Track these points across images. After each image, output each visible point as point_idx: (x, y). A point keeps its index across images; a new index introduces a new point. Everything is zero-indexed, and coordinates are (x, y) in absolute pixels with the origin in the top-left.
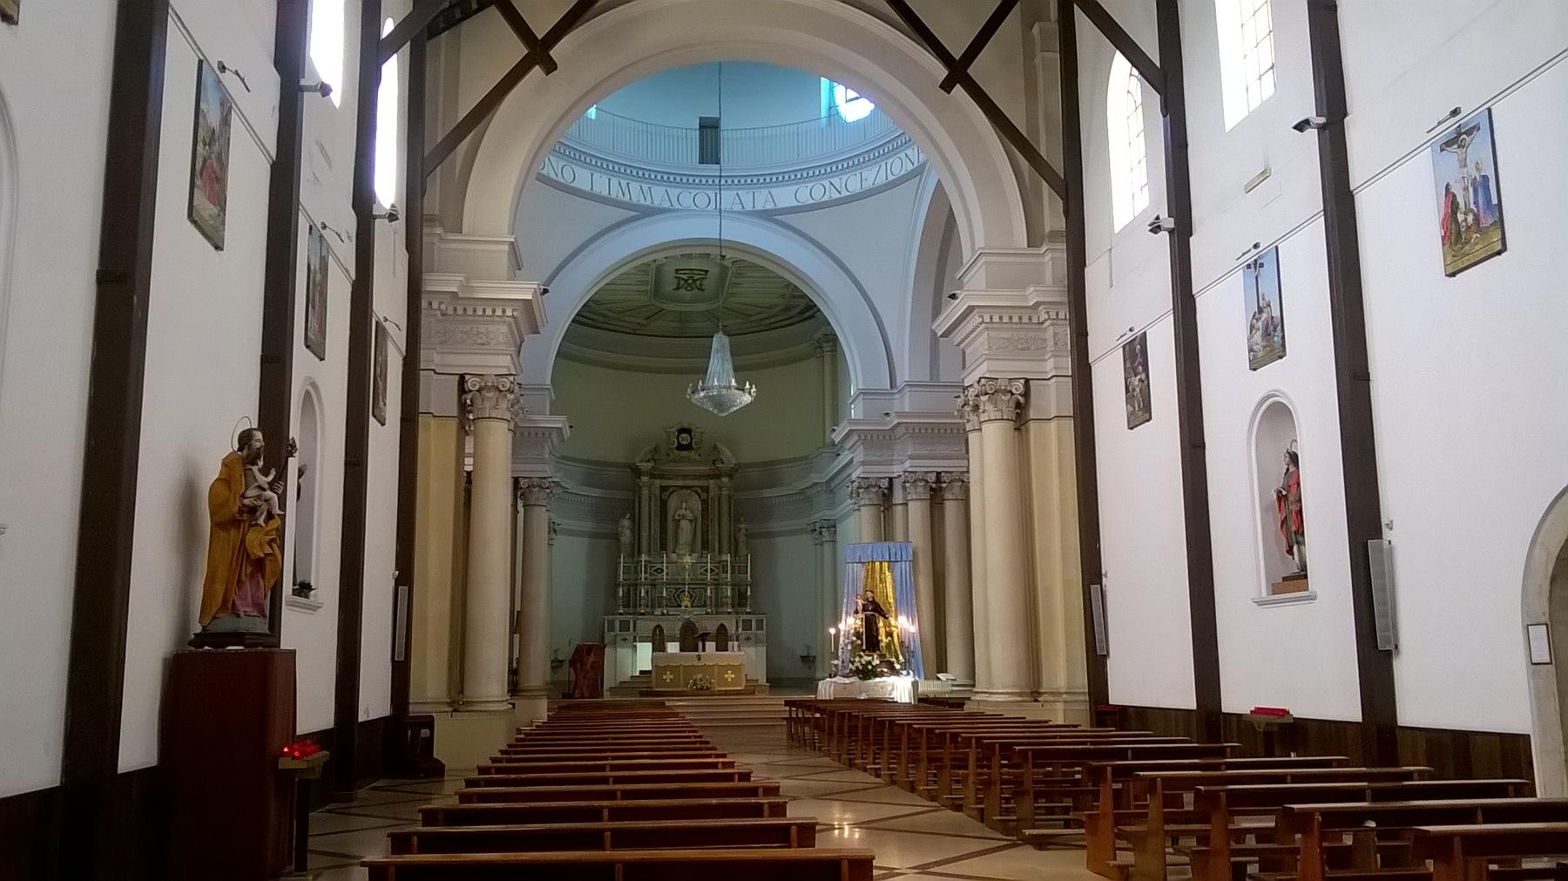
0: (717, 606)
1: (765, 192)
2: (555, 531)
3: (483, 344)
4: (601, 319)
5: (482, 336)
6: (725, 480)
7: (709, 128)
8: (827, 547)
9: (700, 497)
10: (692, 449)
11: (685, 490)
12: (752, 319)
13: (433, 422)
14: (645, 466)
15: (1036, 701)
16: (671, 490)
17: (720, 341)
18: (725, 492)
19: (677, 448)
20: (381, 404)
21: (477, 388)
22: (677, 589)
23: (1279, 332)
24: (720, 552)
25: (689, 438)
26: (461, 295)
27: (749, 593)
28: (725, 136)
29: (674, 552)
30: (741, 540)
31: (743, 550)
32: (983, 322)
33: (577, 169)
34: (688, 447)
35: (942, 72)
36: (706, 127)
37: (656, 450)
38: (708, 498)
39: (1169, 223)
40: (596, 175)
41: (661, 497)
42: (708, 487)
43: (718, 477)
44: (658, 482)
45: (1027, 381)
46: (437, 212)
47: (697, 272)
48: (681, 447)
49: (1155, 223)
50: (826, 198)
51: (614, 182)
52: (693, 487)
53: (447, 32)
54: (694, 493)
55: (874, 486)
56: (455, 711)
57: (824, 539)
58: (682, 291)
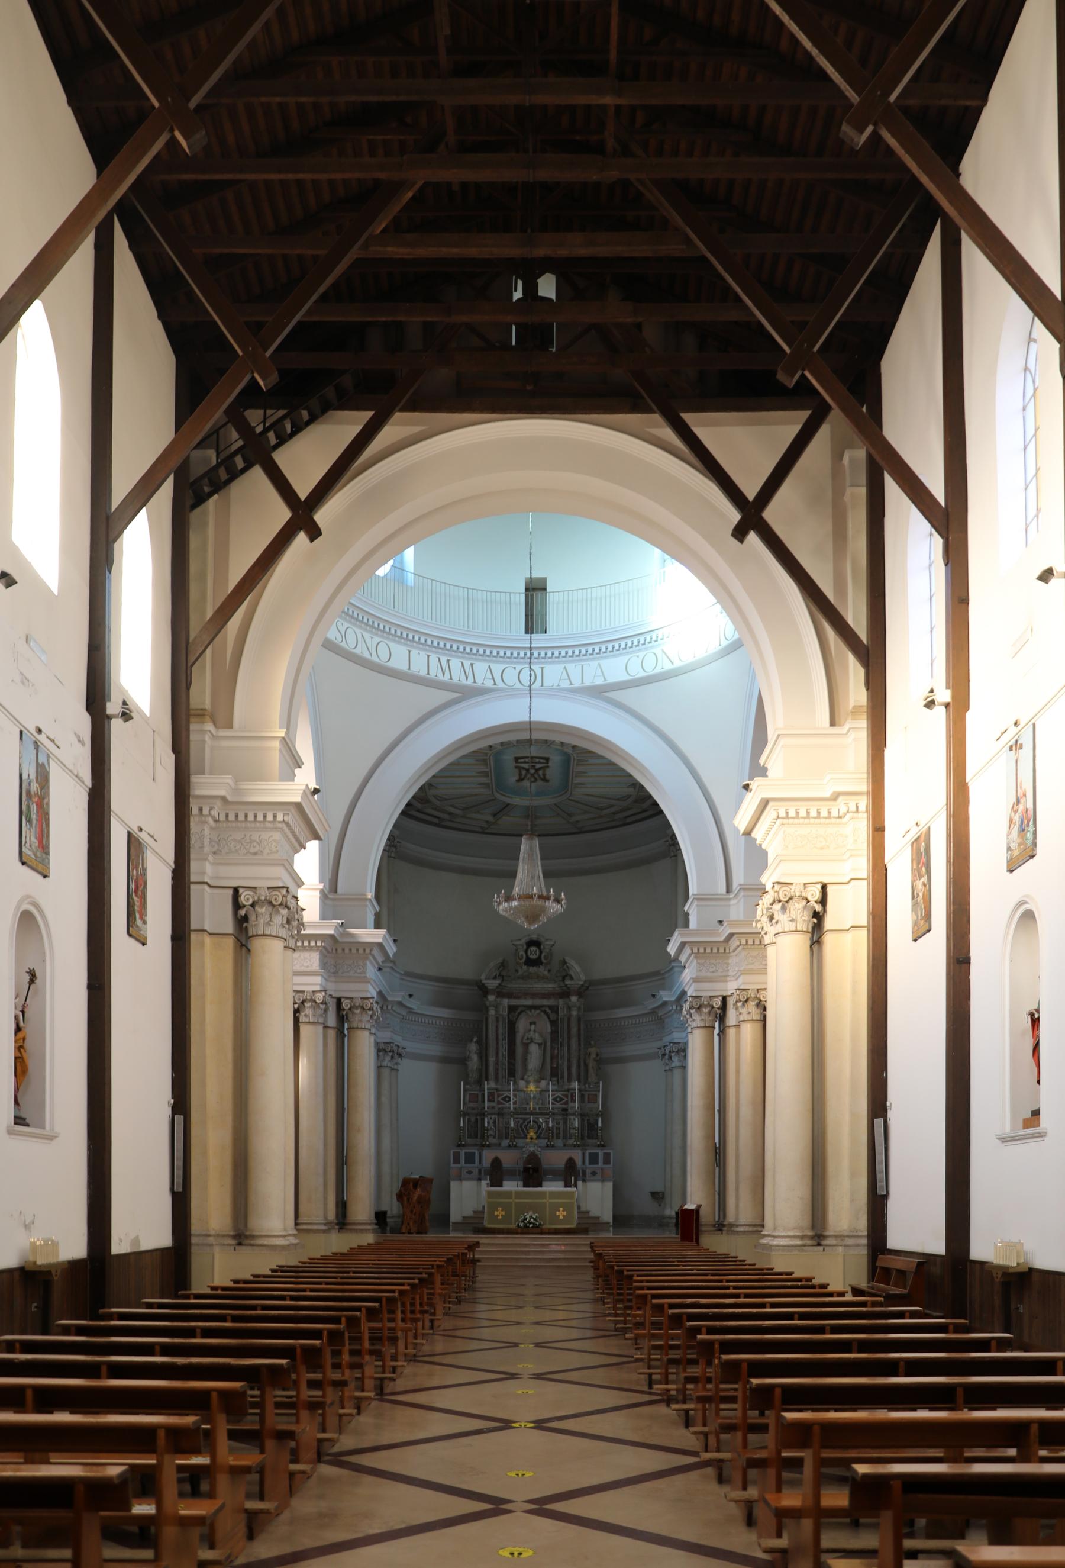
0: (565, 1137)
1: (594, 664)
2: (400, 1055)
3: (255, 854)
4: (446, 817)
5: (255, 844)
6: (574, 999)
7: (535, 589)
8: (677, 1073)
9: (549, 1018)
10: (541, 963)
11: (533, 1011)
12: (605, 812)
13: (208, 940)
14: (492, 984)
15: (819, 1245)
17: (528, 847)
18: (574, 1013)
20: (139, 922)
21: (251, 902)
22: (524, 1120)
23: (1031, 829)
24: (570, 1080)
25: (538, 953)
26: (230, 798)
27: (600, 1124)
28: (552, 597)
29: (522, 1079)
30: (591, 1065)
31: (592, 1077)
32: (778, 818)
33: (392, 645)
34: (537, 962)
35: (734, 516)
36: (534, 589)
37: (503, 965)
39: (944, 695)
40: (414, 652)
41: (509, 1018)
43: (565, 994)
44: (505, 1002)
45: (824, 887)
46: (208, 705)
47: (537, 760)
48: (530, 962)
49: (928, 697)
50: (658, 670)
51: (434, 659)
53: (216, 496)
54: (542, 1014)
55: (706, 1006)
56: (240, 1244)
57: (674, 1065)
58: (526, 783)
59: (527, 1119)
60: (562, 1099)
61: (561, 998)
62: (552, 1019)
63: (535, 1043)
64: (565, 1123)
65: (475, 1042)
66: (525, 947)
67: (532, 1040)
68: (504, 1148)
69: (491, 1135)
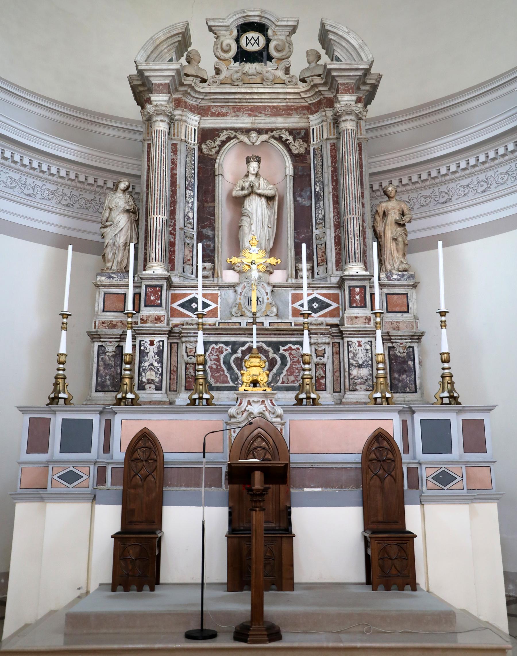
9: (289, 150)
16: (223, 137)
19: (236, 59)
22: (235, 346)
24: (340, 263)
25: (262, 41)
30: (389, 235)
38: (308, 152)
41: (200, 149)
42: (307, 131)
52: (272, 130)
54: (273, 141)
59: (243, 344)
60: (323, 306)
61: (312, 113)
62: (295, 152)
63: (260, 195)
64: (337, 353)
65: (124, 191)
66: (235, 33)
67: (252, 191)
68: (180, 410)
69: (150, 382)
